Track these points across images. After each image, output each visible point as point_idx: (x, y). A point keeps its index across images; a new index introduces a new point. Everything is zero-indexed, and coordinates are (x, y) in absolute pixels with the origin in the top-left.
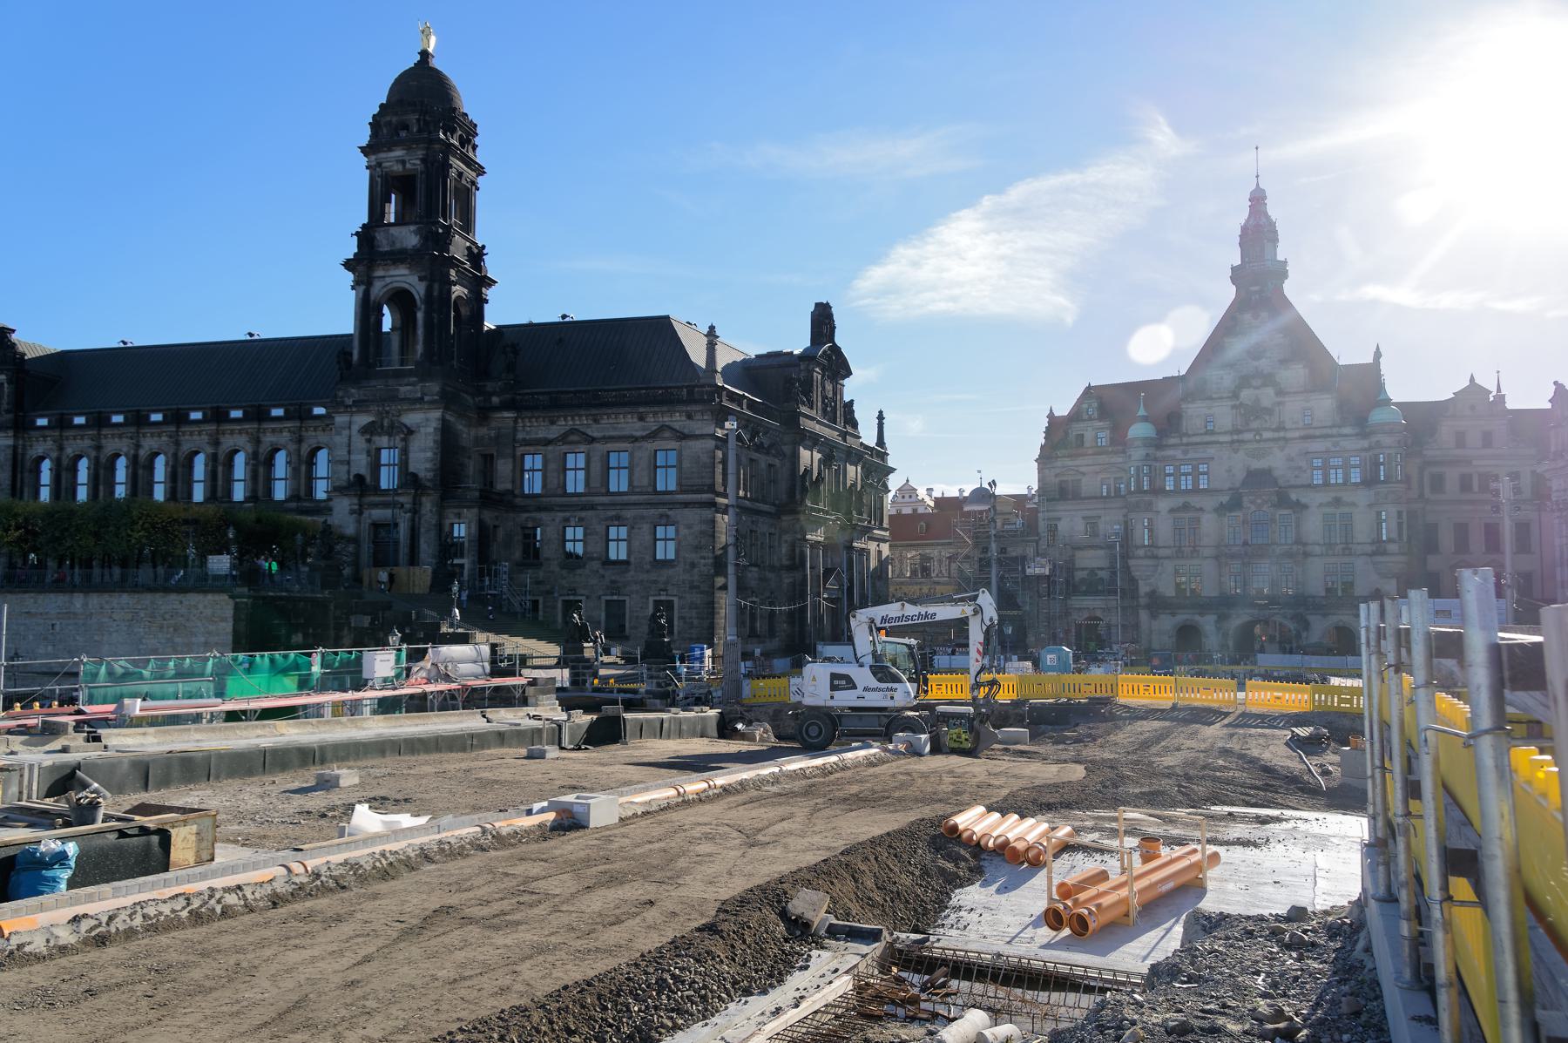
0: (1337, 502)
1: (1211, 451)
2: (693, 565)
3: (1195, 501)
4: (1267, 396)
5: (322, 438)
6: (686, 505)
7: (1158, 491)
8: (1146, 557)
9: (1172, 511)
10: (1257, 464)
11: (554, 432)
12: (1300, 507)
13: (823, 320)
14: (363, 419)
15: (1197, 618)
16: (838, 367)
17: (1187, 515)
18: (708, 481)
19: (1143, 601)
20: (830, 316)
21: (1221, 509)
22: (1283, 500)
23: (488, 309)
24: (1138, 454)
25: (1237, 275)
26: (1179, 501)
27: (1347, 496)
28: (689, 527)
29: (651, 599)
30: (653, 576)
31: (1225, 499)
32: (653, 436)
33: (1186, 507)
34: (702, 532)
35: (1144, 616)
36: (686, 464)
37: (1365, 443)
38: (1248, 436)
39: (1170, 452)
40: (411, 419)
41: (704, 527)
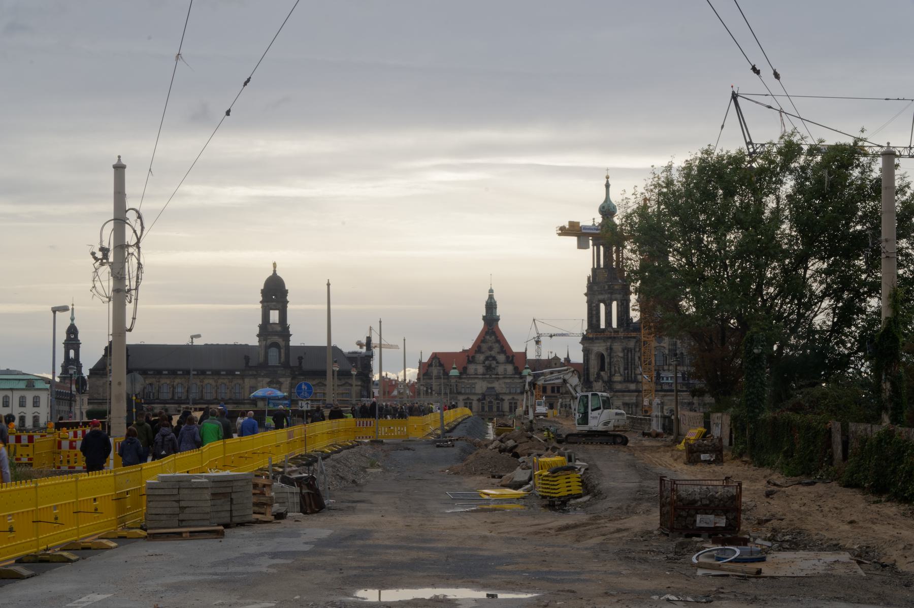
0: (513, 398)
1: (476, 381)
3: (471, 397)
4: (494, 364)
5: (240, 381)
7: (460, 393)
10: (490, 386)
11: (315, 382)
12: (503, 400)
14: (268, 380)
21: (479, 400)
22: (498, 397)
24: (453, 381)
25: (484, 318)
26: (466, 397)
27: (516, 397)
33: (468, 399)
40: (281, 380)
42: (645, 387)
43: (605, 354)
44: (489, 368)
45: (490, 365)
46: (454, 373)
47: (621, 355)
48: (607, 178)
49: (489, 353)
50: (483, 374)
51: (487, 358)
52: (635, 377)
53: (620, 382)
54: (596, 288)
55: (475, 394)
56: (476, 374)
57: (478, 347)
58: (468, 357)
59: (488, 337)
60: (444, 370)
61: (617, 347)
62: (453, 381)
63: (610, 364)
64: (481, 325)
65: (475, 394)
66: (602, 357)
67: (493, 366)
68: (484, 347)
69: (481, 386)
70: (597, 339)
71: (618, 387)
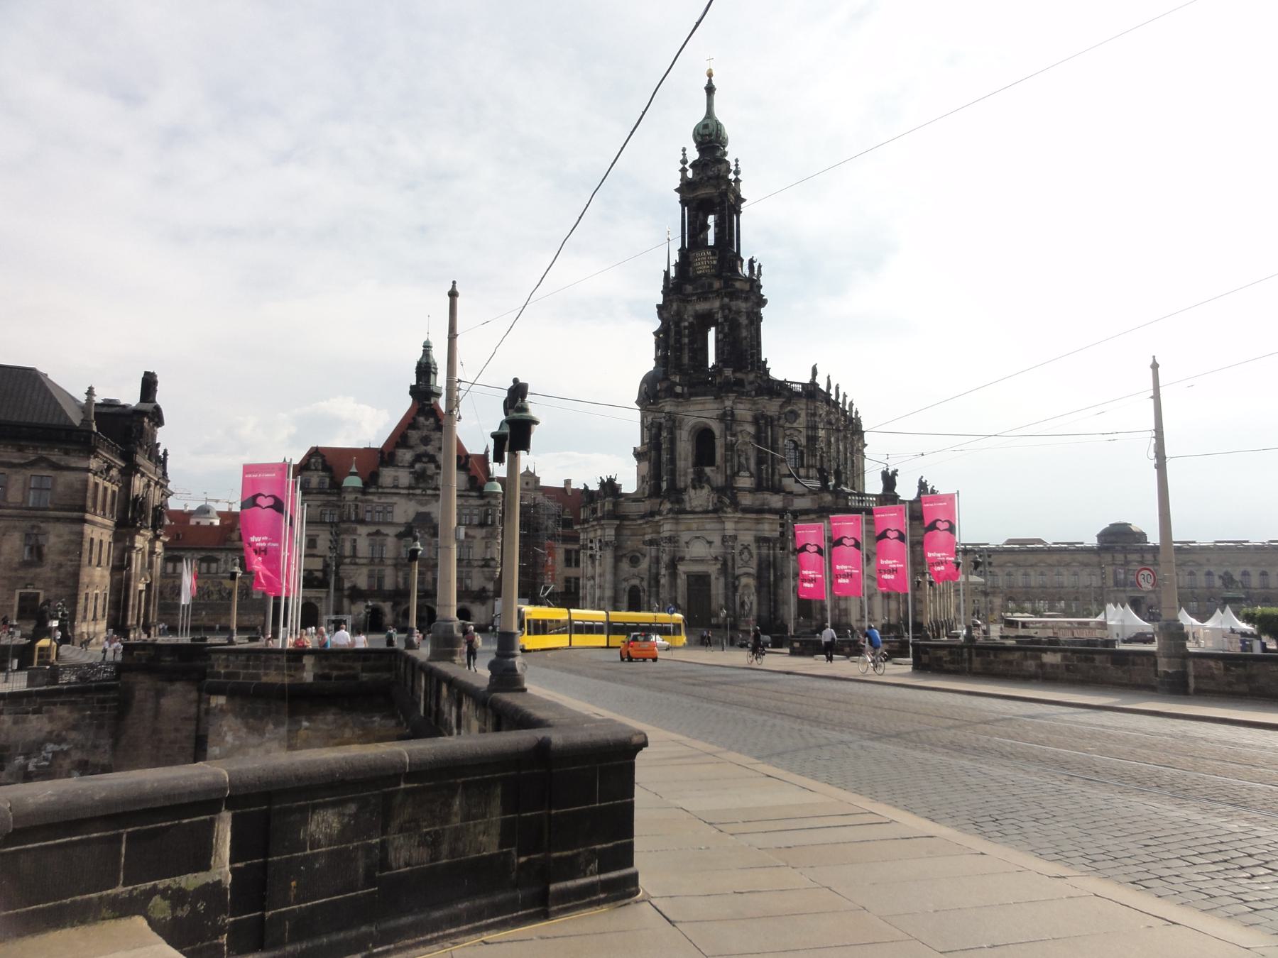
1: (395, 499)
2: (60, 566)
3: (384, 530)
6: (58, 519)
7: (362, 522)
8: (351, 564)
9: (369, 535)
13: (149, 384)
15: (381, 604)
16: (157, 417)
17: (378, 538)
18: (80, 503)
19: (346, 593)
20: (155, 383)
21: (400, 536)
23: (77, 397)
25: (414, 391)
28: (59, 536)
29: (18, 592)
30: (21, 573)
31: (402, 529)
32: (32, 464)
33: (378, 533)
34: (72, 541)
35: (346, 602)
36: (60, 489)
37: (481, 502)
38: (419, 491)
39: (370, 497)
41: (73, 537)
42: (800, 503)
43: (716, 427)
44: (421, 477)
45: (424, 470)
46: (353, 482)
47: (751, 429)
48: (710, 75)
49: (422, 449)
50: (410, 488)
51: (418, 458)
52: (780, 481)
53: (751, 491)
54: (689, 289)
55: (391, 524)
56: (396, 487)
57: (400, 438)
58: (385, 456)
59: (422, 419)
60: (332, 478)
61: (744, 411)
62: (350, 497)
63: (730, 447)
64: (407, 402)
65: (391, 524)
66: (704, 438)
67: (429, 473)
68: (414, 435)
69: (404, 510)
70: (691, 395)
71: (746, 500)
